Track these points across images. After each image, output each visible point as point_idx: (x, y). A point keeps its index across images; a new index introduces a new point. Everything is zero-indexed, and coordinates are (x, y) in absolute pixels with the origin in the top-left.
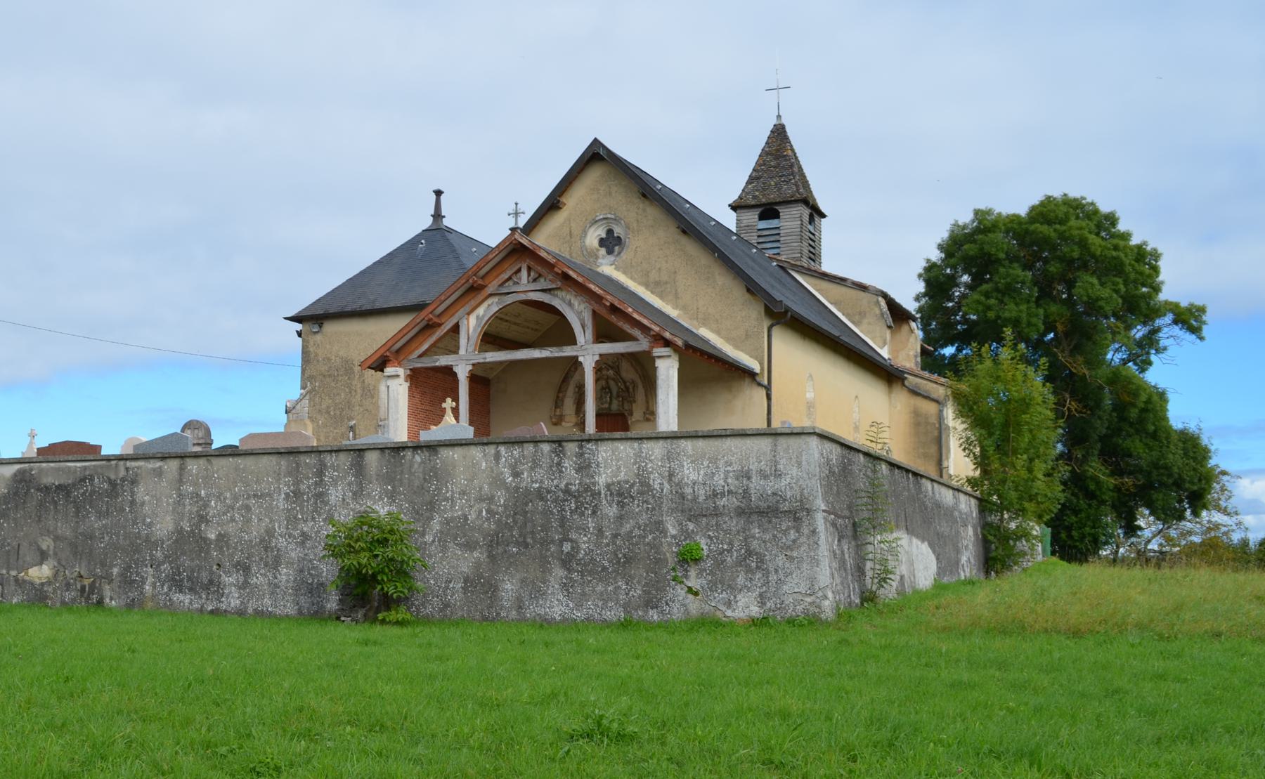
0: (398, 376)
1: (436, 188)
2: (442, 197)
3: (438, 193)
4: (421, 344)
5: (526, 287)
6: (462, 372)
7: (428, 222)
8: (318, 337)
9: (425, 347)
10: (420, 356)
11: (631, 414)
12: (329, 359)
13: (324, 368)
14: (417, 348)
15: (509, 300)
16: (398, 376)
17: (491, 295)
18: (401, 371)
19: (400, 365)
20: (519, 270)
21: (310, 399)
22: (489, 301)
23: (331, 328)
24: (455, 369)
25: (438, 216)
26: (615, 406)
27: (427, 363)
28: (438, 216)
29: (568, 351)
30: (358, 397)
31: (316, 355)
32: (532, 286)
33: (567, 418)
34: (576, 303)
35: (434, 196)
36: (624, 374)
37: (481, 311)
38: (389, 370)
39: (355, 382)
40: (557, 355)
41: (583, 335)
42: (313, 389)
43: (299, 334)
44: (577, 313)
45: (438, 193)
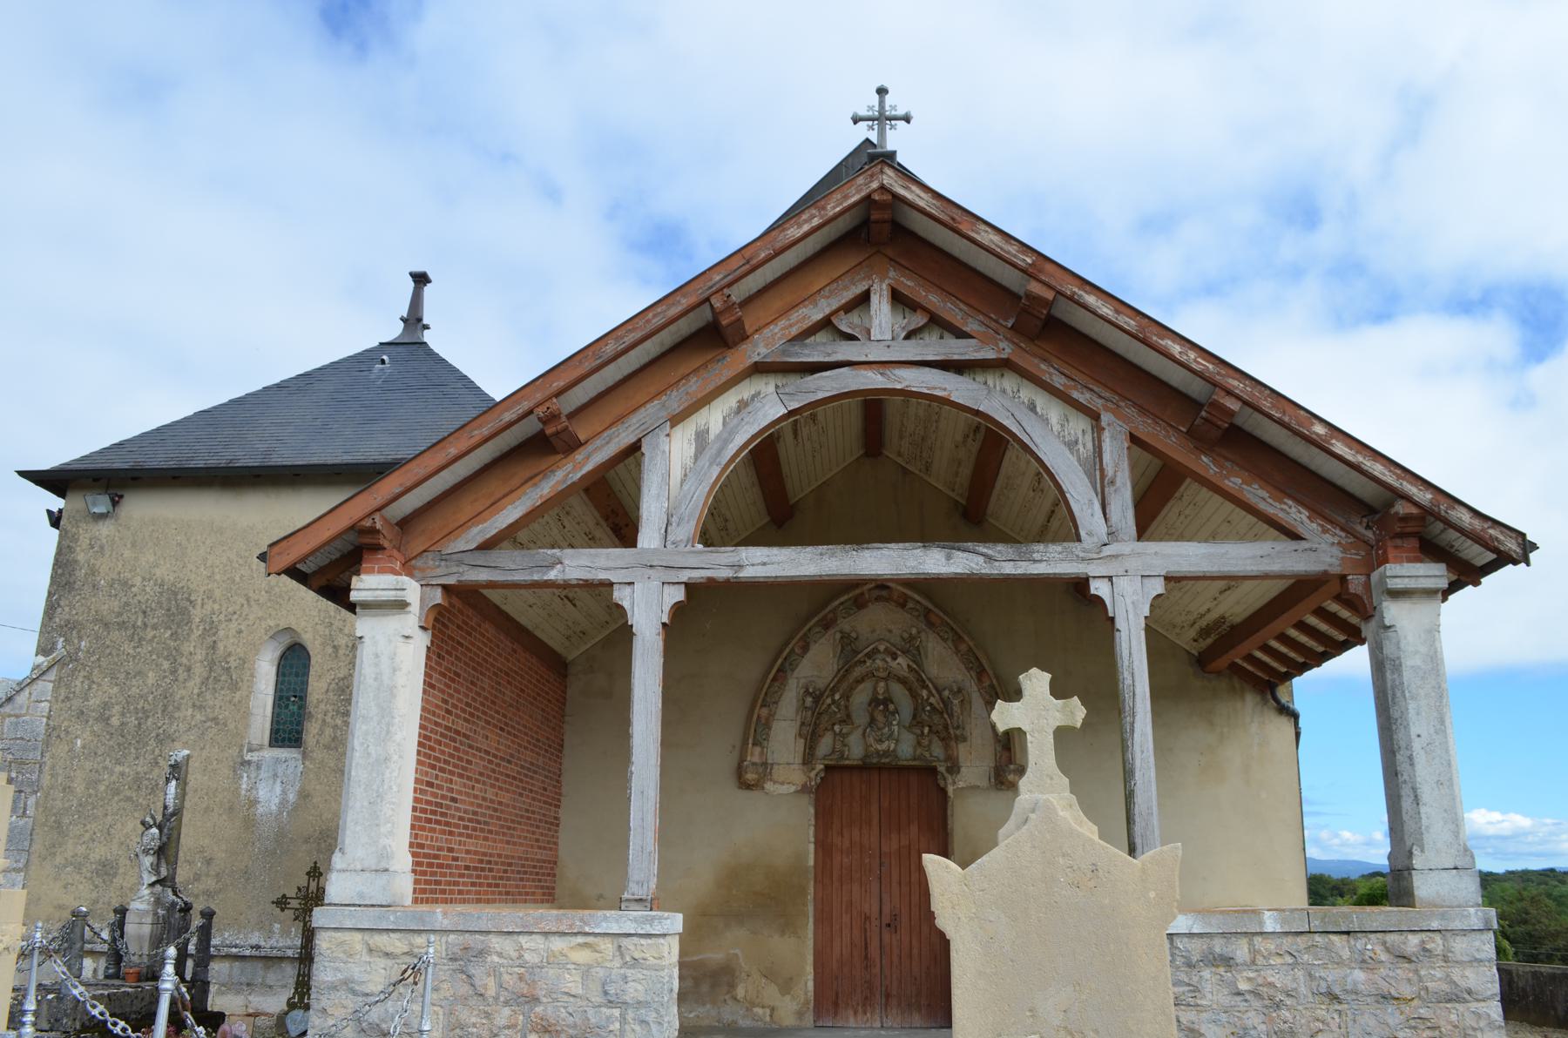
0: (401, 605)
1: (418, 269)
2: (428, 289)
3: (421, 279)
4: (495, 505)
5: (885, 346)
6: (648, 608)
7: (394, 331)
8: (105, 530)
9: (511, 513)
10: (487, 546)
11: (954, 768)
12: (126, 585)
13: (108, 606)
14: (477, 518)
15: (825, 385)
16: (401, 605)
17: (761, 369)
18: (412, 590)
19: (408, 569)
20: (864, 299)
21: (58, 683)
22: (745, 390)
23: (142, 509)
24: (621, 596)
25: (414, 320)
26: (906, 748)
27: (511, 567)
28: (414, 320)
29: (1051, 561)
30: (194, 685)
31: (93, 571)
32: (912, 351)
33: (778, 773)
34: (1054, 411)
35: (410, 284)
36: (933, 669)
37: (714, 417)
38: (367, 585)
39: (187, 647)
40: (1008, 569)
41: (1099, 507)
42: (72, 657)
43: (55, 520)
44: (1057, 435)
45: (421, 279)
